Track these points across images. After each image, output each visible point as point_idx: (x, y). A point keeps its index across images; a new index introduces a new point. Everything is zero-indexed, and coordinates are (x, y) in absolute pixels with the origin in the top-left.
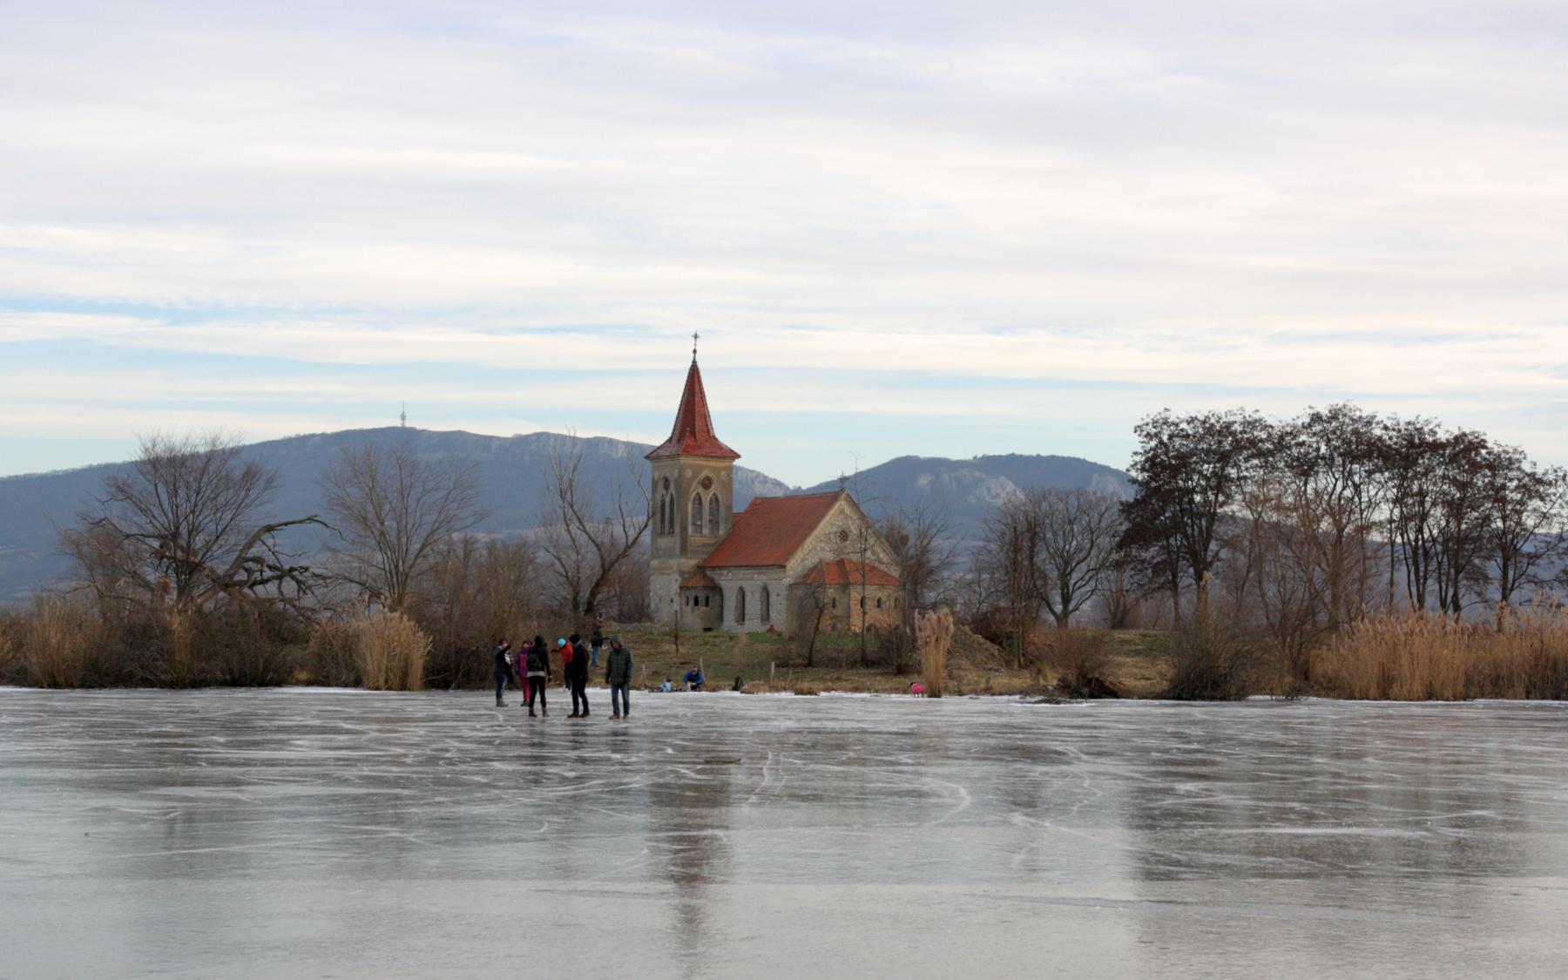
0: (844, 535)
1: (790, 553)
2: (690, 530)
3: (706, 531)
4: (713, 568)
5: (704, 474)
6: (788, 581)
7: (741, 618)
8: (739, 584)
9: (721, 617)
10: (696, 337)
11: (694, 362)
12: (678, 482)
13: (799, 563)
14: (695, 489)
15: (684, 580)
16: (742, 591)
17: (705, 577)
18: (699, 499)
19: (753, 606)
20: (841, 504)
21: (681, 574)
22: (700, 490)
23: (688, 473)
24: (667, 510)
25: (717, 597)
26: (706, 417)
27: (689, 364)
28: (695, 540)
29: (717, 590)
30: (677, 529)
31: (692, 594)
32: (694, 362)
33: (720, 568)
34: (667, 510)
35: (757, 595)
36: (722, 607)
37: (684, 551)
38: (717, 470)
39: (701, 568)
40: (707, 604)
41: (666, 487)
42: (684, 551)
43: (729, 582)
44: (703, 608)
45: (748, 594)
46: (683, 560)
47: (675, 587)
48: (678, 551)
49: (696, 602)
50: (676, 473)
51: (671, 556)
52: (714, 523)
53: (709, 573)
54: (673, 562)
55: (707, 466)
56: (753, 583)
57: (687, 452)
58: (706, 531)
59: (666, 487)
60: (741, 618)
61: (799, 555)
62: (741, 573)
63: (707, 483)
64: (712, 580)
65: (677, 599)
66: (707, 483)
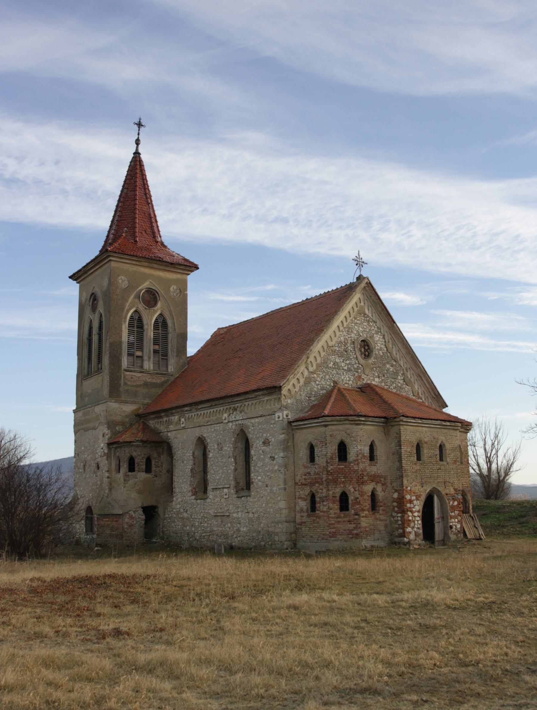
0: (366, 348)
1: (286, 368)
2: (125, 361)
3: (149, 365)
4: (158, 414)
5: (146, 284)
6: (284, 415)
7: (202, 488)
8: (197, 433)
9: (169, 488)
10: (139, 125)
11: (137, 154)
12: (107, 294)
13: (301, 384)
14: (131, 307)
15: (115, 433)
16: (202, 443)
17: (146, 428)
18: (137, 323)
19: (222, 468)
20: (357, 296)
21: (111, 424)
22: (141, 307)
23: (123, 281)
24: (95, 338)
25: (164, 458)
26: (151, 219)
27: (131, 156)
28: (132, 378)
29: (164, 446)
30: (106, 360)
31: (125, 453)
32: (137, 154)
33: (169, 411)
34: (95, 338)
35: (228, 448)
36: (171, 472)
37: (115, 391)
38: (168, 283)
39: (141, 417)
40: (148, 470)
41: (94, 308)
42: (115, 391)
43: (181, 433)
44: (143, 475)
45: (212, 447)
46: (113, 405)
47: (102, 444)
48: (106, 391)
49: (132, 468)
50: (105, 284)
51: (97, 403)
52: (161, 354)
53: (152, 423)
54: (99, 409)
55: (152, 277)
56: (218, 428)
57: (122, 253)
58: (149, 365)
59: (94, 308)
60: (202, 488)
61: (302, 371)
62: (204, 414)
63: (151, 298)
64: (157, 433)
65: (104, 463)
66: (151, 298)
